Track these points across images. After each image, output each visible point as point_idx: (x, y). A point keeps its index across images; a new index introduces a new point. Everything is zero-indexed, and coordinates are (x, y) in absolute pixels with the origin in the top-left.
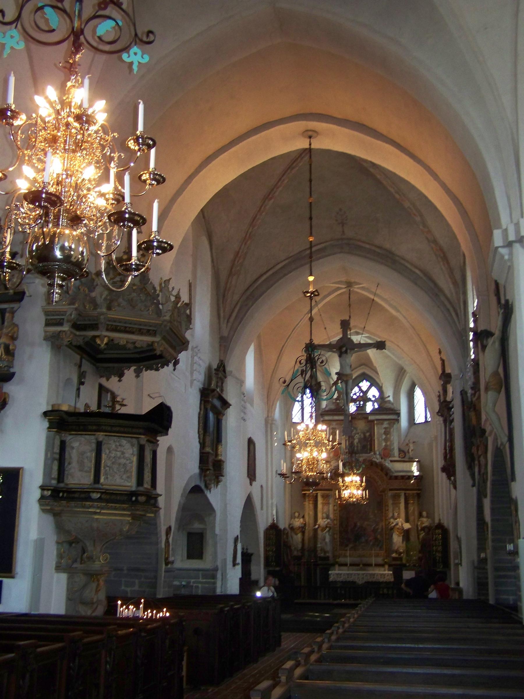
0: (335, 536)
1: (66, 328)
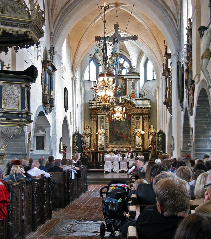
0: (107, 138)
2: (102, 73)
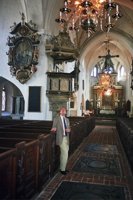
1: (51, 51)
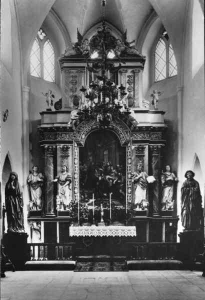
2: (66, 55)
